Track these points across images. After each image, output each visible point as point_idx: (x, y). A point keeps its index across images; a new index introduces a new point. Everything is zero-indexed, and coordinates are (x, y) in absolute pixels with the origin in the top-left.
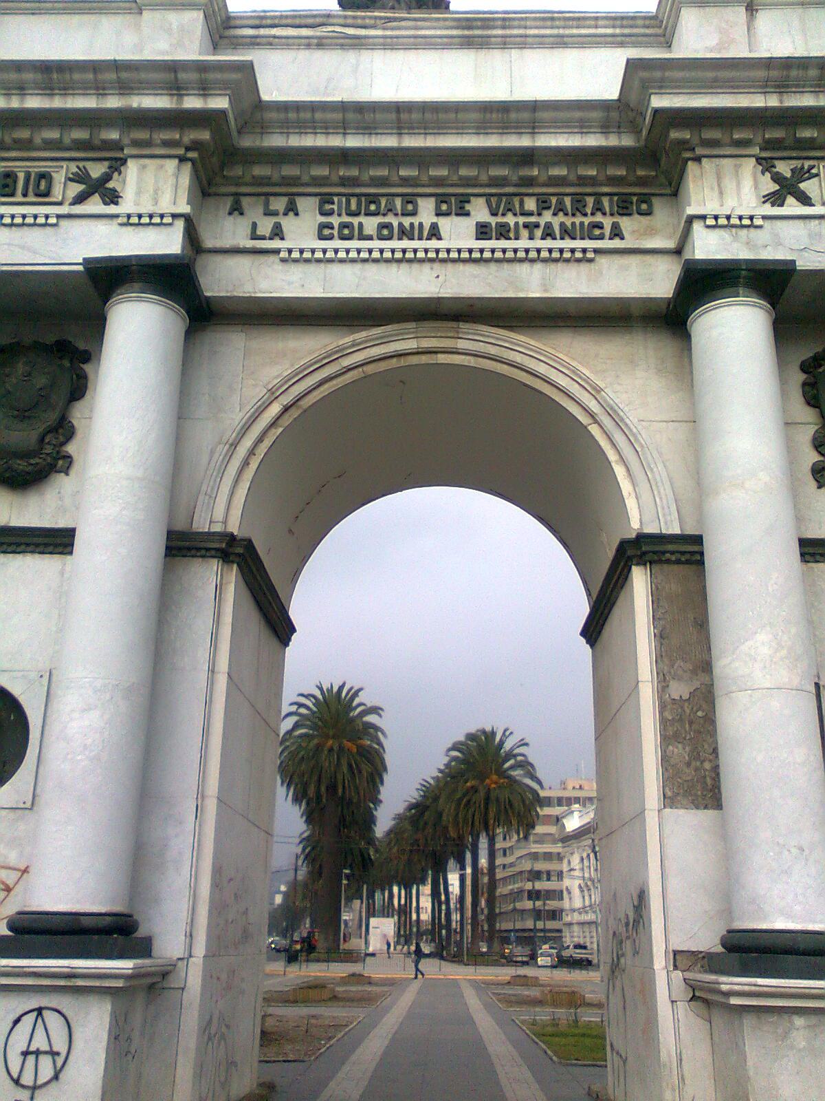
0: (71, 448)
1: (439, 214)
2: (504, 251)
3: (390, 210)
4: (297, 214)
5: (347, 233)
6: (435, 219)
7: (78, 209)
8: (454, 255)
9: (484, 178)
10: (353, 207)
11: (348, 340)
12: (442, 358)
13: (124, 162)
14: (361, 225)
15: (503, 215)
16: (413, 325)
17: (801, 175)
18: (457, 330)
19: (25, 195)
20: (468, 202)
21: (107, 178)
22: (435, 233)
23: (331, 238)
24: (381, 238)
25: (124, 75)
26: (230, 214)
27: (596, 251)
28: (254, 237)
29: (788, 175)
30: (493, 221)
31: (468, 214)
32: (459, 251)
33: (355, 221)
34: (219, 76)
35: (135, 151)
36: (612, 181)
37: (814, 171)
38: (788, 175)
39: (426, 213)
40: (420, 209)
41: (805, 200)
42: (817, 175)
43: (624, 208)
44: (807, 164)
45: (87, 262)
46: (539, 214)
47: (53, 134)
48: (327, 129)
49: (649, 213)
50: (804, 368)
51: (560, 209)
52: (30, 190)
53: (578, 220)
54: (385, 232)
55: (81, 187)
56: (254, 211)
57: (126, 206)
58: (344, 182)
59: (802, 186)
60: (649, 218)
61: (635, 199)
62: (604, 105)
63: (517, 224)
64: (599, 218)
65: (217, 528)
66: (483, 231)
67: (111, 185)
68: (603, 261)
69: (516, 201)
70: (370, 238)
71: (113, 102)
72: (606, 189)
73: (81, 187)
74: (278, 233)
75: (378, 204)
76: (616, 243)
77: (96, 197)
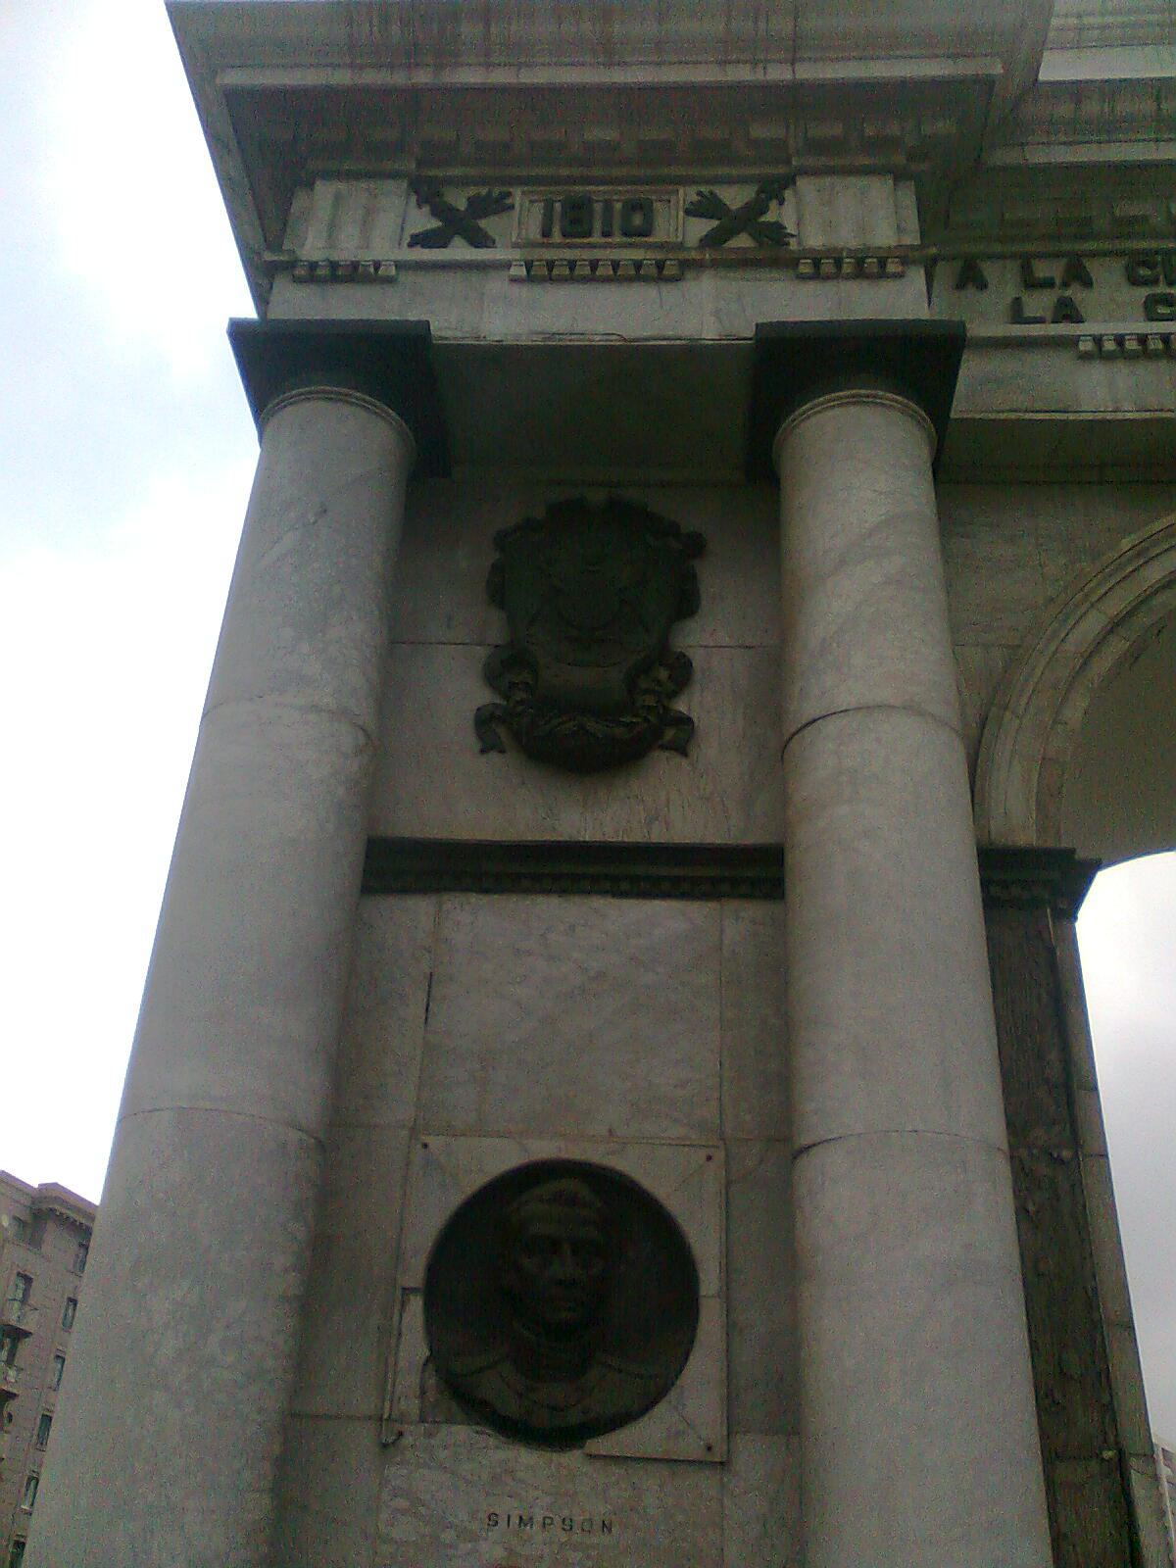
4: (1087, 283)
13: (789, 181)
19: (606, 234)
21: (757, 207)
35: (811, 161)
67: (769, 217)
71: (779, 73)
74: (1067, 312)
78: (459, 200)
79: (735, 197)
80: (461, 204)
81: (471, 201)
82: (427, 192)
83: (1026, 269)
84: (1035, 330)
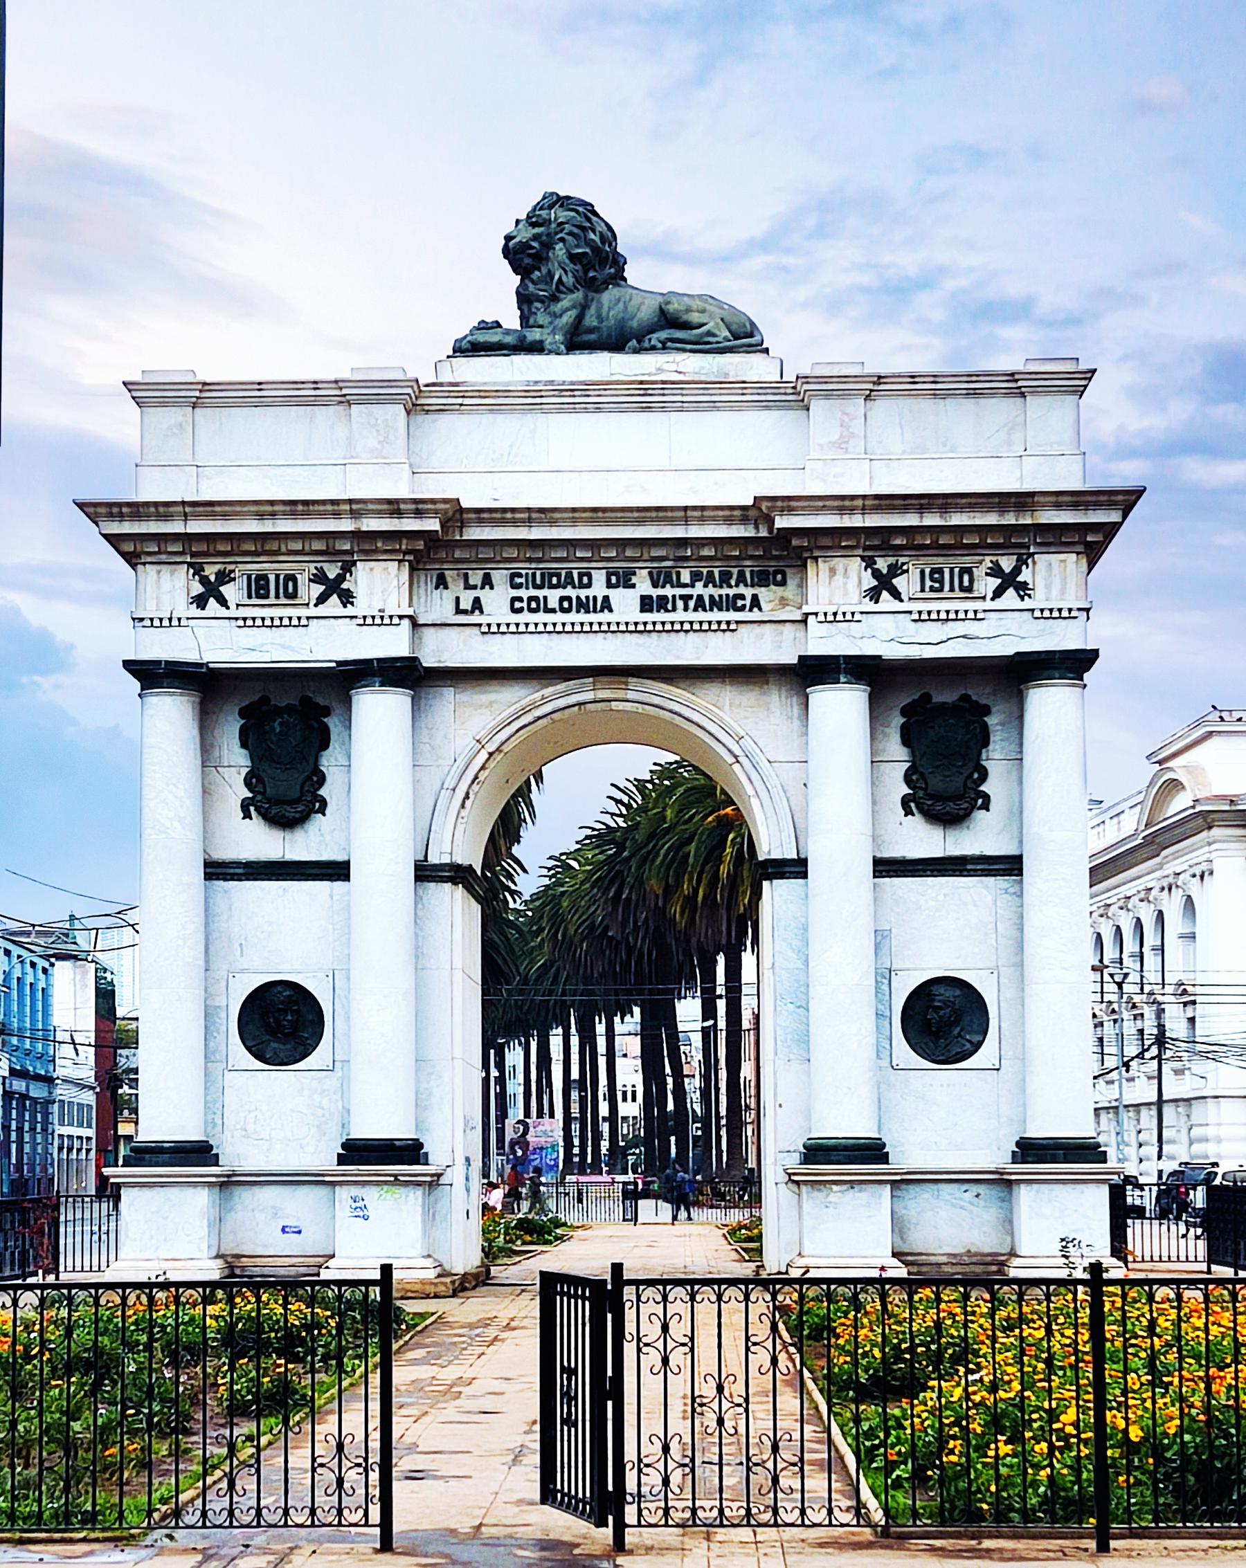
0: (322, 792)
1: (609, 585)
2: (663, 623)
3: (569, 581)
4: (492, 588)
5: (537, 605)
7: (322, 610)
8: (623, 628)
9: (646, 556)
10: (538, 581)
11: (538, 695)
12: (613, 703)
13: (354, 563)
14: (545, 598)
15: (663, 587)
16: (591, 680)
17: (895, 570)
18: (626, 683)
19: (277, 597)
20: (634, 574)
21: (341, 578)
22: (607, 605)
23: (521, 610)
24: (563, 610)
25: (354, 507)
26: (437, 588)
27: (737, 622)
28: (459, 611)
29: (885, 571)
30: (655, 593)
31: (633, 586)
32: (627, 624)
34: (430, 506)
36: (752, 557)
37: (905, 567)
38: (885, 571)
39: (598, 589)
40: (594, 581)
41: (896, 595)
42: (907, 571)
43: (763, 579)
44: (902, 560)
45: (339, 663)
46: (693, 586)
47: (297, 546)
48: (515, 523)
49: (783, 583)
50: (903, 713)
51: (710, 580)
52: (281, 591)
53: (725, 591)
54: (566, 605)
55: (322, 588)
56: (456, 588)
57: (362, 606)
58: (530, 560)
59: (895, 581)
60: (782, 588)
61: (771, 569)
62: (744, 508)
63: (674, 596)
64: (742, 590)
65: (446, 860)
66: (646, 604)
67: (345, 586)
68: (743, 629)
69: (674, 571)
70: (553, 611)
71: (346, 525)
72: (748, 563)
73: (322, 588)
75: (558, 576)
76: (756, 615)
77: (334, 599)
78: (211, 572)
79: (332, 572)
80: (212, 578)
81: (218, 574)
82: (198, 569)
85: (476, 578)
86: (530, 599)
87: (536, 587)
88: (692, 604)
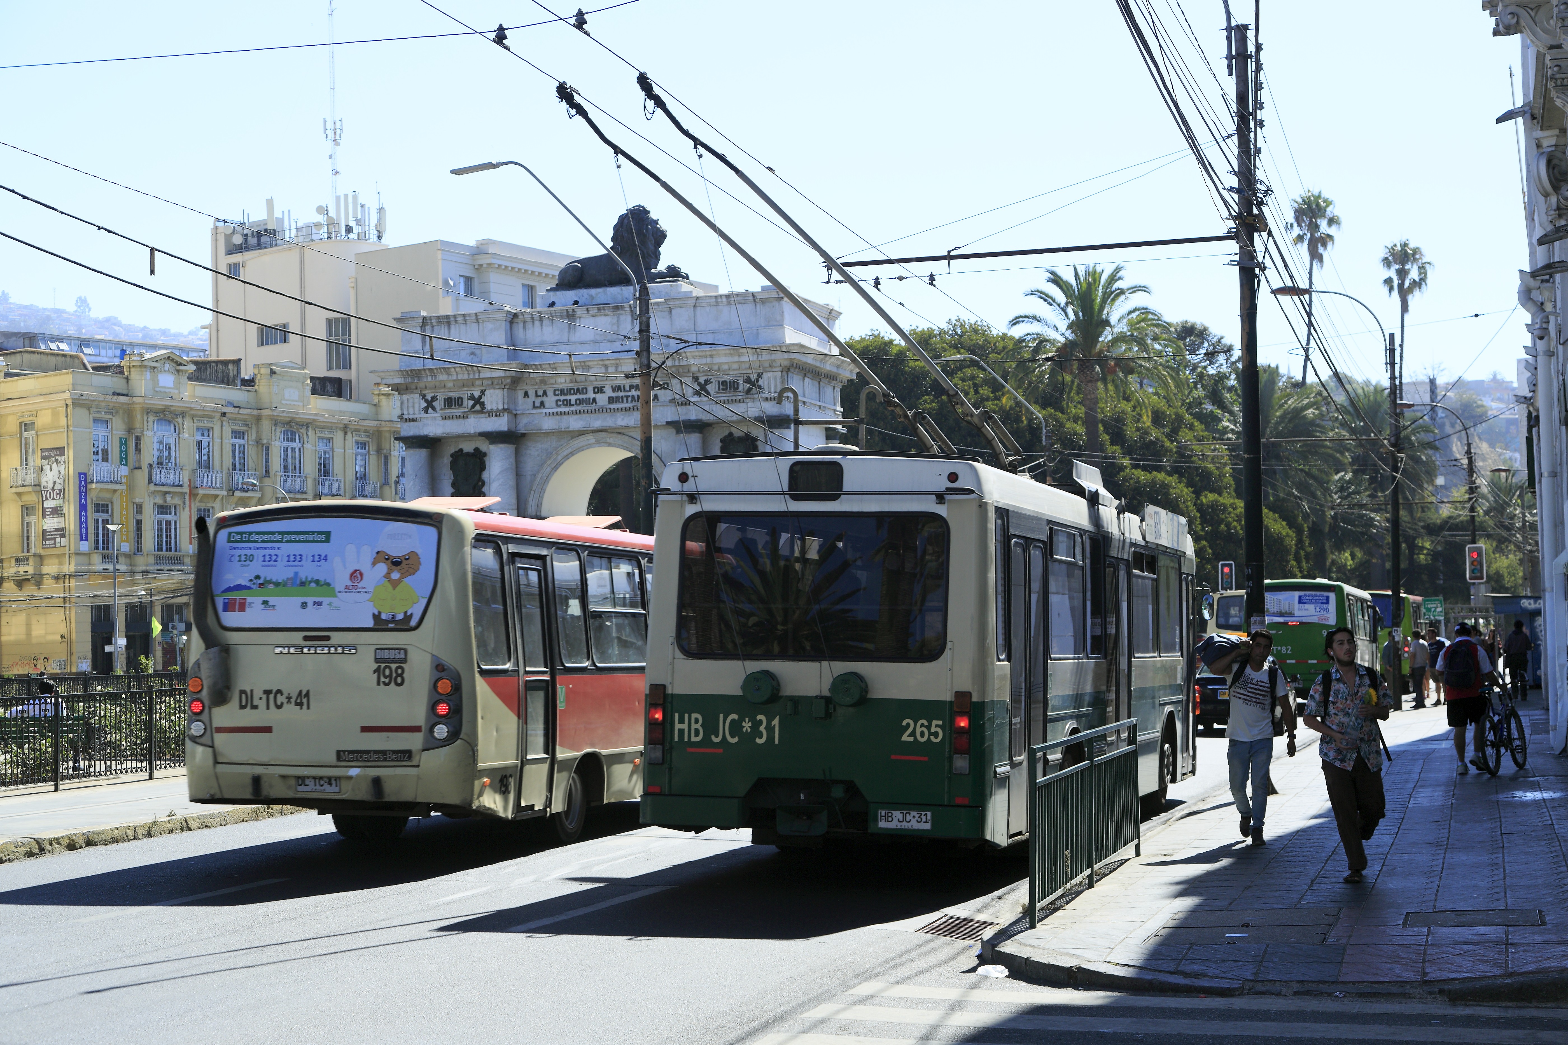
1: (595, 393)
6: (593, 396)
21: (480, 397)
28: (535, 407)
33: (568, 397)
78: (429, 398)
82: (424, 397)
83: (536, 392)
84: (535, 411)
85: (540, 393)
86: (564, 400)
87: (565, 395)
88: (630, 399)
